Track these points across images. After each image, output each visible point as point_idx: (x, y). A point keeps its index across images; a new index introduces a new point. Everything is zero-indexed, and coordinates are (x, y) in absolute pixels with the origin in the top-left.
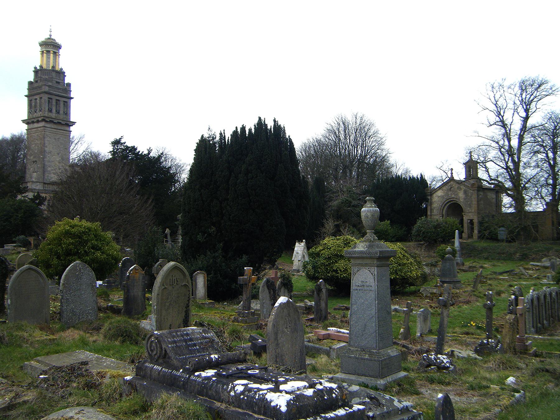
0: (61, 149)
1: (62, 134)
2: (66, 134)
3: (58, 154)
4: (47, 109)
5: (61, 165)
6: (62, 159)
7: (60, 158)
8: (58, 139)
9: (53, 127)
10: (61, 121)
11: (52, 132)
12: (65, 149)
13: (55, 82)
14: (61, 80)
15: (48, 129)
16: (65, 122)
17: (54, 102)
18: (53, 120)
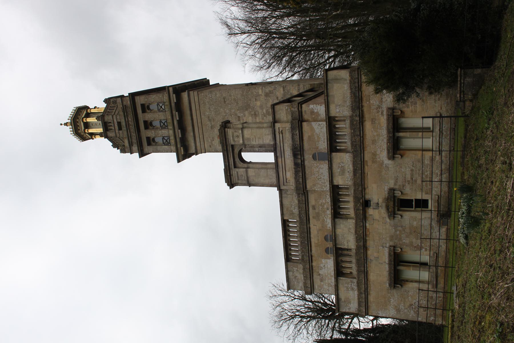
0: (227, 111)
1: (198, 112)
2: (197, 104)
3: (239, 117)
4: (166, 147)
5: (260, 111)
6: (247, 109)
7: (246, 113)
8: (210, 120)
9: (192, 134)
10: (176, 123)
11: (201, 136)
12: (225, 102)
13: (121, 132)
14: (113, 121)
15: (198, 144)
16: (174, 112)
17: (151, 133)
18: (178, 140)
